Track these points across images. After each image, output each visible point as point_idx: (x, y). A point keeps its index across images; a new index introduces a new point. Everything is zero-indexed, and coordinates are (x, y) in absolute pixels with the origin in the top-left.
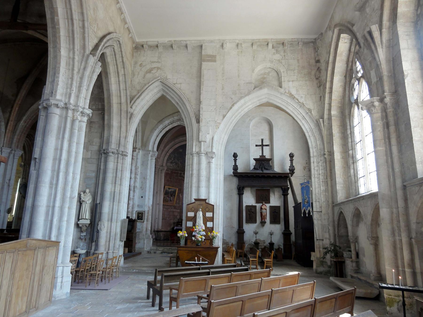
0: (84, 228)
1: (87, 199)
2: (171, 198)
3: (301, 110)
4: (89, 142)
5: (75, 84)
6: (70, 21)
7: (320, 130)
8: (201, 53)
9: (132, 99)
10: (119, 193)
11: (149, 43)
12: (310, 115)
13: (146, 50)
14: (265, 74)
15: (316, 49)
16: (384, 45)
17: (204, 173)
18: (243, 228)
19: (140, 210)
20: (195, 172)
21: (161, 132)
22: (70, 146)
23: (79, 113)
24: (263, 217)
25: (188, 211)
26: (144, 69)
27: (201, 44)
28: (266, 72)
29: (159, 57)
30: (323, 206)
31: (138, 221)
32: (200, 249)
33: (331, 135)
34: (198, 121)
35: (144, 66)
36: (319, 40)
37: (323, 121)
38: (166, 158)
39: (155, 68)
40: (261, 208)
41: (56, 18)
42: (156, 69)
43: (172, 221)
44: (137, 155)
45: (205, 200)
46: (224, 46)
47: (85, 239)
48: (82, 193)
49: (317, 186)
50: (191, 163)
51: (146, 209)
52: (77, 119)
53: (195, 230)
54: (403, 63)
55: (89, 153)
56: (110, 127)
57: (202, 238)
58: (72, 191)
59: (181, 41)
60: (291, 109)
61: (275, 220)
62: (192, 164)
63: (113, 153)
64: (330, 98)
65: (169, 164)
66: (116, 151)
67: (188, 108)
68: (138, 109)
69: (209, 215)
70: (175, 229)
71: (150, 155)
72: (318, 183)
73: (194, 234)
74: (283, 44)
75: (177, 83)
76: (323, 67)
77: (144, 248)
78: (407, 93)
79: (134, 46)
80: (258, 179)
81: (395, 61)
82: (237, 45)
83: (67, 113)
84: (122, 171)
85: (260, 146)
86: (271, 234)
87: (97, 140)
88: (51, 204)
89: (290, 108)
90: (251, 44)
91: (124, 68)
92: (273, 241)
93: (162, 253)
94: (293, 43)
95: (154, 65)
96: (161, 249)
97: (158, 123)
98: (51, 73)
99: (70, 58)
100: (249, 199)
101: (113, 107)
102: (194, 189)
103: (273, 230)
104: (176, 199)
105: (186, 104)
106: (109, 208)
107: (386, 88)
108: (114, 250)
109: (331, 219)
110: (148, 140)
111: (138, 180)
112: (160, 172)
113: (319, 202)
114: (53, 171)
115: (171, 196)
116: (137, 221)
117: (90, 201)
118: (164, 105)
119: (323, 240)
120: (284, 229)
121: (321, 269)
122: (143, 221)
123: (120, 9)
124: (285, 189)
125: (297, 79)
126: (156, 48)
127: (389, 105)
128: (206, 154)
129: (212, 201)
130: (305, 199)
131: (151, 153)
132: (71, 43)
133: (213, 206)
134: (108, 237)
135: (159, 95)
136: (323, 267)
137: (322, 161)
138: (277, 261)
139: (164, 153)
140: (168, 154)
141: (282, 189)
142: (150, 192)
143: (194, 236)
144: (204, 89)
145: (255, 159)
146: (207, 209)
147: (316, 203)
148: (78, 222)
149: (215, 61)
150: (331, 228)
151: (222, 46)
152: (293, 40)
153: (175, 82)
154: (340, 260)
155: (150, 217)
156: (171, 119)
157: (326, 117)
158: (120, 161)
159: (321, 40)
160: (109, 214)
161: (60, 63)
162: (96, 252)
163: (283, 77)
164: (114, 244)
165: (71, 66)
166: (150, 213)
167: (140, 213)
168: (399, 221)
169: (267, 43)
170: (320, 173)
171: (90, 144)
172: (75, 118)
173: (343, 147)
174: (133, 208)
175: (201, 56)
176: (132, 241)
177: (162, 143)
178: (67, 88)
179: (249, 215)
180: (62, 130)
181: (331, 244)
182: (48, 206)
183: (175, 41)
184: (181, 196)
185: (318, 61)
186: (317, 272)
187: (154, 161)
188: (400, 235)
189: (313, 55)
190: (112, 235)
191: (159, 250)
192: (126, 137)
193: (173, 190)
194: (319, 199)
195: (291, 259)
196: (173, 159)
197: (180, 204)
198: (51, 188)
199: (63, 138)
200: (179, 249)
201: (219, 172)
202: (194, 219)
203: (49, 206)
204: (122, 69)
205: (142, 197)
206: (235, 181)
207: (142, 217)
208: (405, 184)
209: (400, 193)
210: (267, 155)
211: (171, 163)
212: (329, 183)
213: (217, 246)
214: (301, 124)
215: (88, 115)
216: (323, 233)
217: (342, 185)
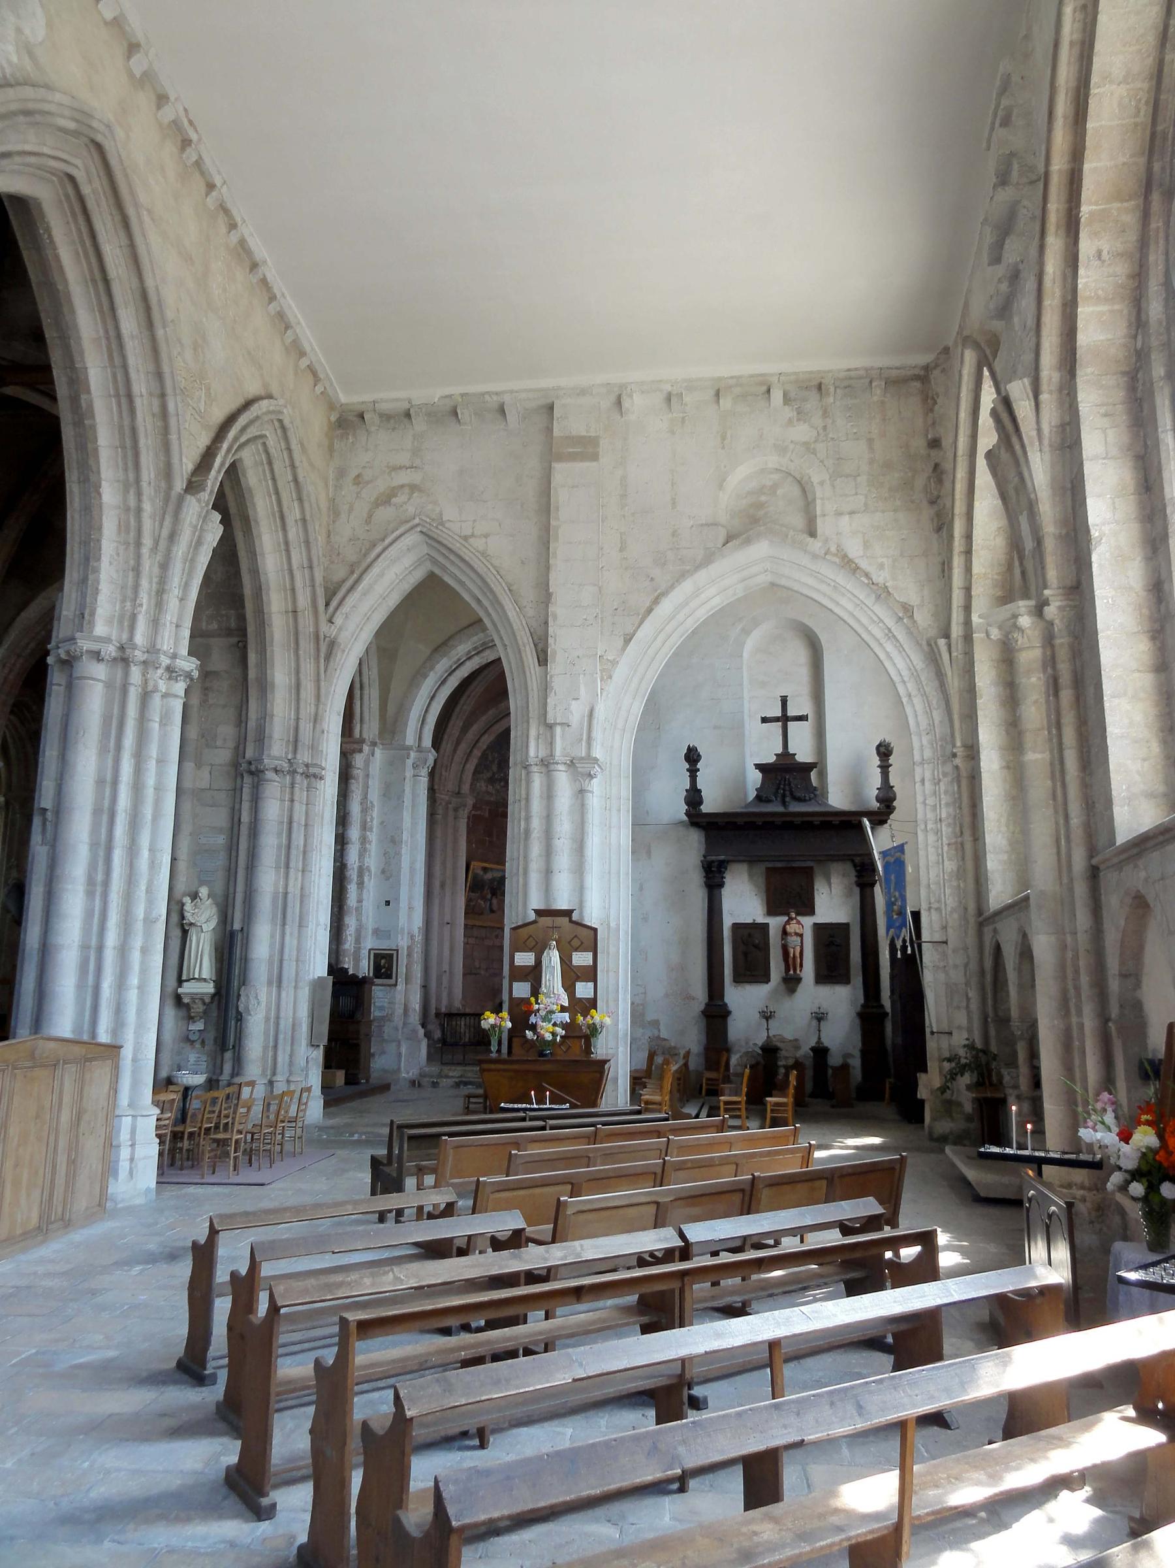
0: (199, 1008)
1: (203, 918)
2: (495, 901)
3: (880, 610)
4: (203, 737)
5: (146, 585)
6: (124, 400)
7: (940, 675)
8: (549, 430)
9: (332, 595)
10: (302, 896)
11: (384, 407)
12: (910, 625)
13: (373, 429)
14: (761, 490)
15: (929, 401)
16: (1046, 442)
17: (564, 827)
19: (384, 945)
20: (536, 824)
21: (444, 682)
22: (138, 771)
23: (160, 671)
24: (791, 962)
25: (516, 948)
26: (370, 494)
27: (549, 401)
28: (764, 486)
29: (416, 452)
30: (950, 924)
31: (377, 981)
32: (547, 1067)
33: (971, 691)
34: (543, 659)
35: (368, 483)
36: (936, 372)
37: (949, 646)
38: (471, 767)
39: (402, 486)
40: (785, 933)
41: (83, 397)
42: (406, 490)
44: (367, 763)
45: (568, 913)
46: (626, 404)
47: (203, 1042)
48: (187, 900)
49: (933, 858)
50: (524, 796)
51: (403, 943)
52: (155, 690)
53: (537, 1007)
54: (1091, 503)
55: (205, 773)
56: (264, 686)
57: (554, 1034)
58: (150, 902)
59: (483, 394)
60: (850, 607)
61: (831, 969)
62: (527, 799)
63: (276, 771)
64: (968, 569)
65: (482, 786)
66: (286, 765)
67: (512, 614)
68: (351, 626)
69: (581, 959)
71: (409, 762)
72: (937, 848)
73: (533, 1019)
74: (819, 387)
75: (473, 535)
76: (947, 466)
77: (399, 1069)
78: (1097, 593)
79: (333, 419)
80: (778, 832)
81: (1072, 490)
82: (669, 398)
83: (126, 674)
84: (306, 825)
85: (776, 719)
86: (820, 1017)
87: (226, 732)
88: (94, 942)
89: (843, 601)
90: (713, 392)
91: (300, 499)
92: (826, 1042)
93: (457, 1085)
94: (852, 384)
95: (403, 478)
96: (455, 1072)
98: (76, 556)
99: (128, 509)
100: (743, 902)
101: (270, 626)
102: (535, 879)
105: (504, 603)
106: (272, 945)
107: (1052, 574)
108: (291, 1074)
109: (974, 966)
110: (403, 710)
111: (373, 847)
112: (451, 813)
113: (938, 910)
114: (94, 845)
116: (373, 984)
117: (213, 924)
118: (437, 607)
119: (951, 1033)
121: (944, 1126)
122: (392, 981)
123: (281, 315)
125: (866, 505)
126: (406, 420)
127: (1058, 625)
128: (571, 764)
129: (592, 915)
130: (894, 904)
131: (412, 754)
132: (130, 464)
133: (595, 930)
134: (272, 1033)
135: (419, 575)
136: (953, 1119)
137: (949, 778)
138: (833, 1107)
140: (477, 753)
141: (855, 866)
142: (412, 883)
143: (533, 1028)
144: (560, 550)
145: (760, 767)
146: (576, 943)
147: (930, 915)
148: (180, 990)
149: (594, 457)
150: (973, 994)
151: (619, 402)
152: (852, 373)
153: (469, 533)
154: (989, 1095)
156: (475, 638)
157: (956, 631)
158: (300, 795)
159: (943, 371)
160: (271, 962)
161: (100, 528)
162: (237, 1080)
163: (818, 502)
164: (291, 1056)
165: (132, 534)
167: (383, 956)
168: (1077, 972)
169: (765, 388)
170: (944, 815)
171: (207, 746)
172: (150, 688)
173: (1008, 733)
174: (358, 940)
175: (550, 438)
176: (357, 1046)
177: (454, 717)
178: (123, 601)
179: (746, 954)
180: (114, 724)
181: (970, 1047)
182: (85, 947)
183: (462, 395)
185: (935, 444)
186: (931, 1138)
187: (424, 781)
188: (1079, 1013)
189: (919, 422)
190: (282, 1026)
191: (447, 1077)
192: (316, 719)
194: (939, 901)
195: (882, 1099)
196: (495, 768)
198: (90, 894)
199: (119, 747)
200: (485, 1066)
201: (614, 820)
202: (534, 975)
203: (89, 947)
204: (296, 504)
205: (388, 903)
206: (695, 840)
207: (390, 968)
208: (1094, 861)
209: (1081, 889)
210: (803, 752)
212: (968, 846)
213: (604, 1058)
214: (882, 656)
215: (188, 675)
216: (949, 1013)
217: (1005, 857)
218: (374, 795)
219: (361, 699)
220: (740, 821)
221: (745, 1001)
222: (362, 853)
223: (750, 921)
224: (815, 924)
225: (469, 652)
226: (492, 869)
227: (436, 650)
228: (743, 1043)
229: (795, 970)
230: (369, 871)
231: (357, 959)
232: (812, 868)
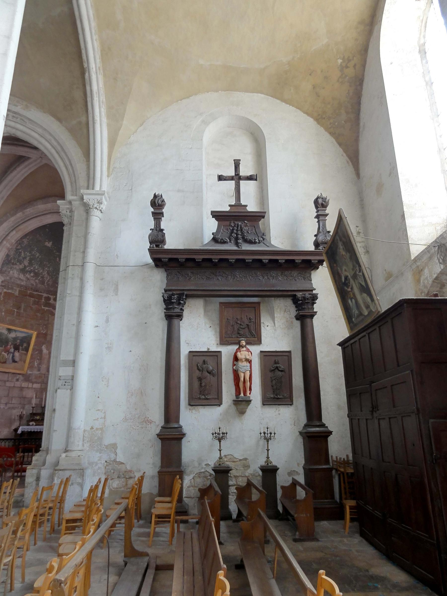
18: (177, 420)
40: (236, 359)
43: (16, 412)
61: (277, 393)
70: (19, 432)
85: (232, 178)
86: (267, 437)
92: (275, 462)
100: (199, 331)
103: (270, 425)
115: (16, 348)
120: (303, 420)
124: (304, 298)
145: (216, 215)
179: (200, 379)
184: (45, 351)
196: (26, 263)
206: (159, 279)
211: (23, 271)
220: (199, 258)
221: (198, 423)
223: (206, 350)
224: (261, 352)
226: (15, 331)
228: (196, 464)
229: (245, 394)
232: (259, 303)
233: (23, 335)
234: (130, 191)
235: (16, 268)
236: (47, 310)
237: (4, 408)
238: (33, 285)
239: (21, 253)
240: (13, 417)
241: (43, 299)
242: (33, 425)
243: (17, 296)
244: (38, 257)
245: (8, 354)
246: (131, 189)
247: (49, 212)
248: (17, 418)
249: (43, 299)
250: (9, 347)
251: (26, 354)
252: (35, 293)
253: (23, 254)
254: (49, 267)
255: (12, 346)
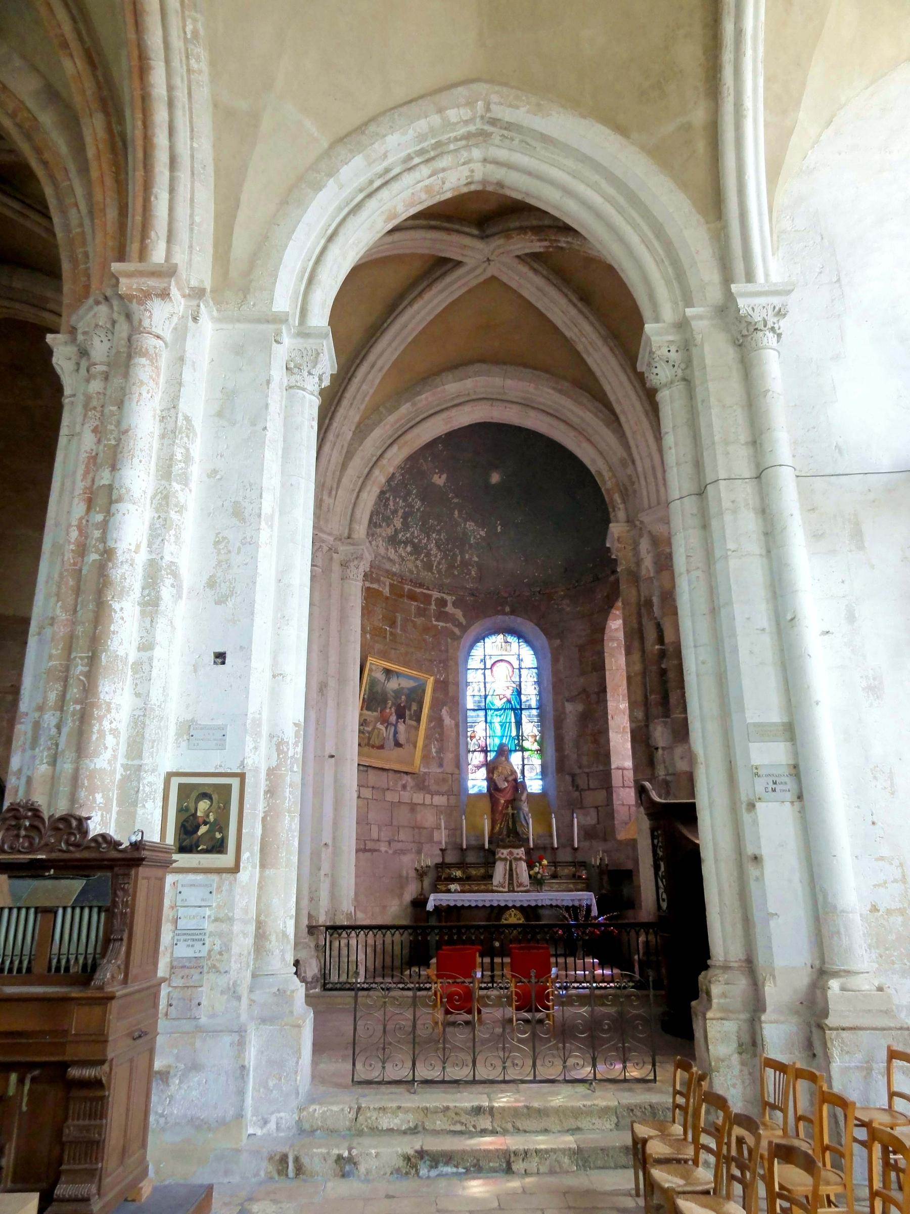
2: (401, 727)
19: (208, 762)
43: (408, 863)
44: (181, 334)
51: (257, 759)
70: (430, 907)
97: (332, 146)
104: (427, 737)
110: (265, 251)
116: (166, 865)
122: (225, 860)
131: (287, 340)
139: (357, 465)
142: (281, 619)
155: (290, 828)
156: (422, 125)
166: (290, 796)
177: (345, 403)
184: (447, 721)
193: (407, 684)
196: (398, 523)
197: (449, 767)
207: (221, 825)
218: (196, 403)
219: (172, 190)
222: (159, 530)
225: (409, 158)
226: (398, 675)
227: (341, 140)
230: (175, 575)
231: (130, 799)
233: (411, 684)
234: (837, 285)
235: (380, 536)
236: (442, 627)
237: (386, 852)
238: (411, 572)
239: (388, 499)
240: (404, 873)
241: (433, 603)
242: (456, 891)
243: (387, 598)
244: (418, 510)
245: (386, 728)
246: (839, 280)
247: (467, 399)
248: (413, 874)
249: (433, 603)
250: (388, 711)
251: (417, 728)
252: (418, 590)
253: (391, 503)
254: (439, 533)
255: (393, 710)
